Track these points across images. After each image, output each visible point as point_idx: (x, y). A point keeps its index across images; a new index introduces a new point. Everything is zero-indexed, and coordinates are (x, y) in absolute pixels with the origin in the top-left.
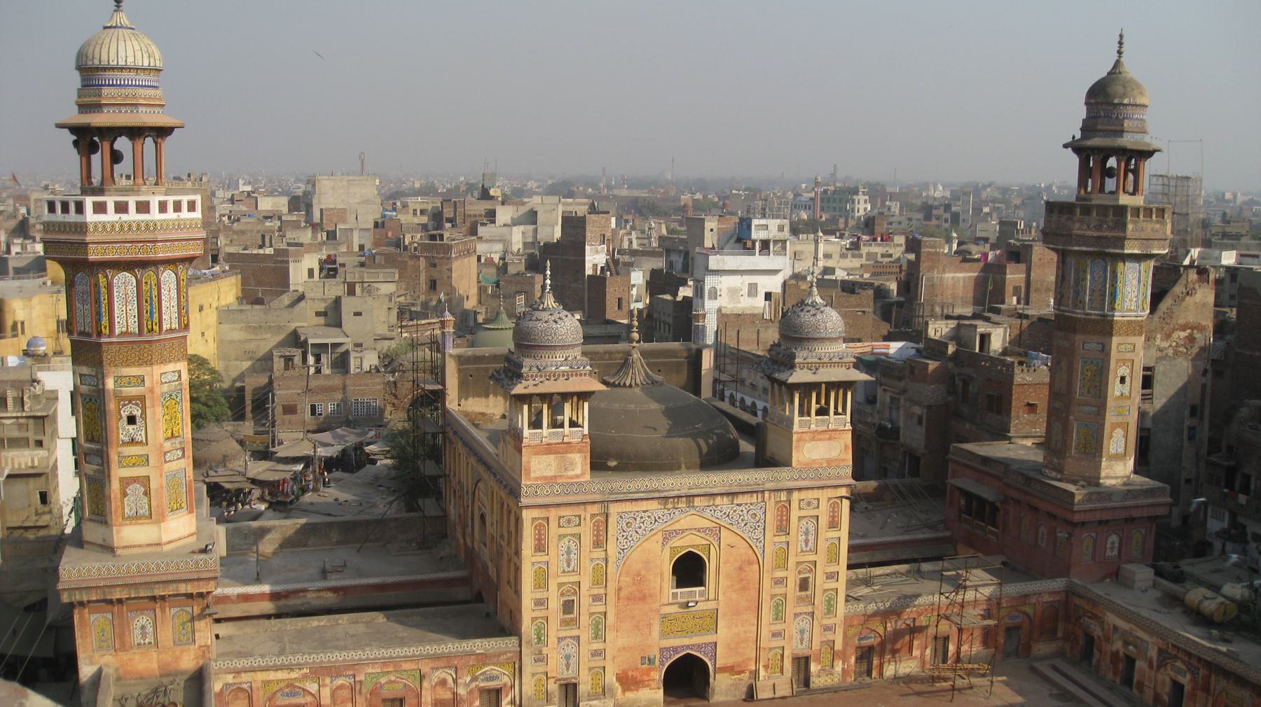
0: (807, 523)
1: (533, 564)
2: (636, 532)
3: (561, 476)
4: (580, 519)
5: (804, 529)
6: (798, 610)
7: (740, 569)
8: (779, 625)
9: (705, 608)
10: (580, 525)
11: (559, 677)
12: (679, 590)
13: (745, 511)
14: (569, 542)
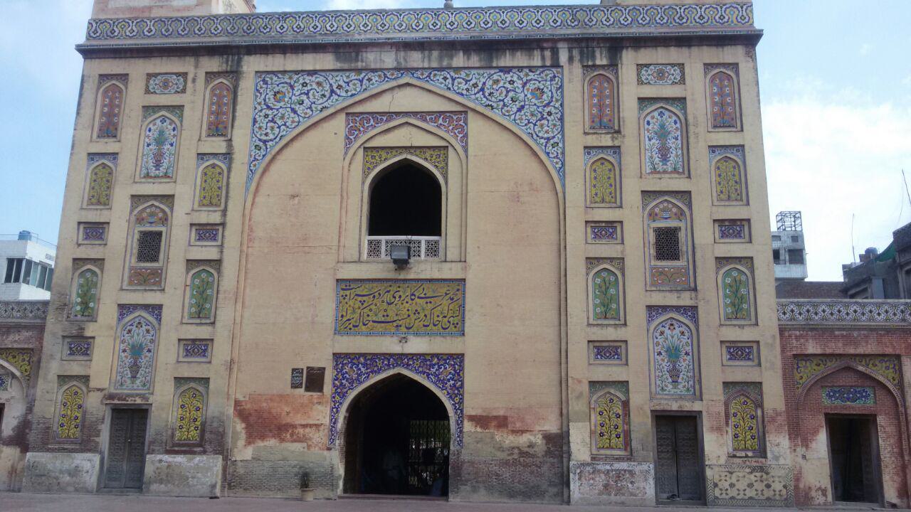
0: (661, 114)
1: (92, 156)
2: (294, 111)
3: (162, 7)
4: (185, 81)
5: (654, 126)
6: (658, 299)
7: (516, 198)
8: (611, 330)
9: (437, 275)
10: (184, 91)
11: (113, 391)
12: (383, 238)
13: (518, 84)
14: (163, 121)
